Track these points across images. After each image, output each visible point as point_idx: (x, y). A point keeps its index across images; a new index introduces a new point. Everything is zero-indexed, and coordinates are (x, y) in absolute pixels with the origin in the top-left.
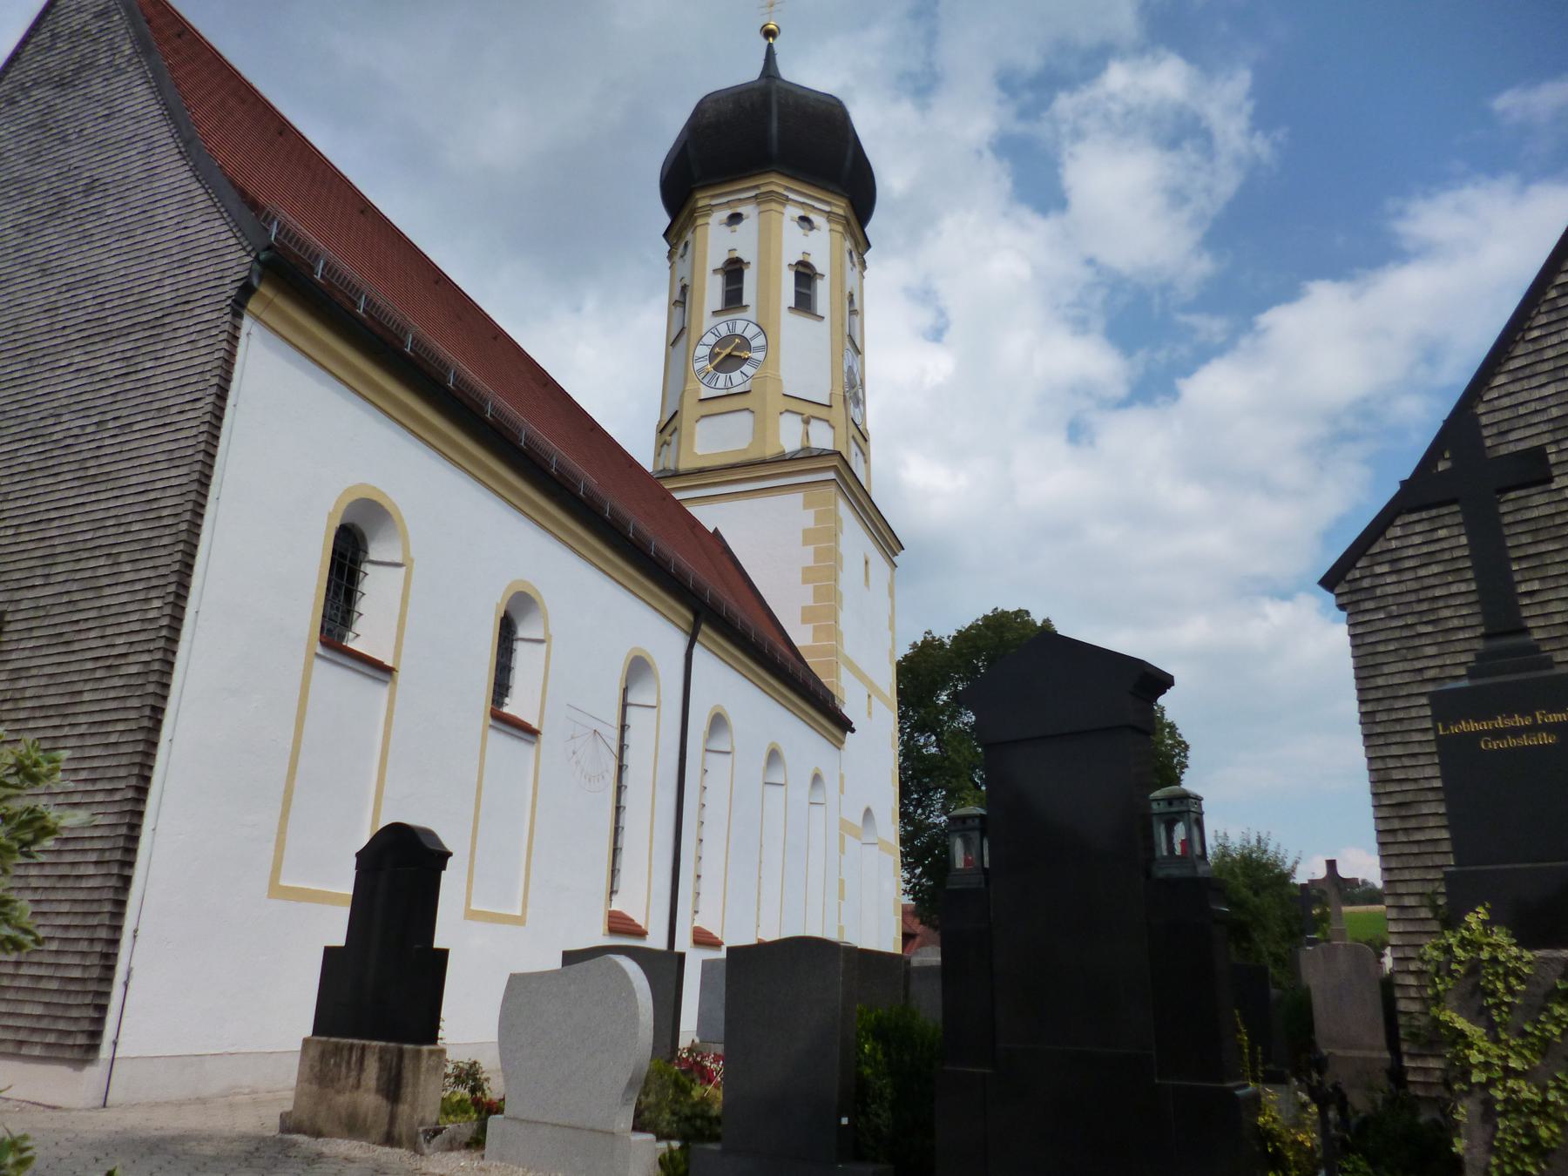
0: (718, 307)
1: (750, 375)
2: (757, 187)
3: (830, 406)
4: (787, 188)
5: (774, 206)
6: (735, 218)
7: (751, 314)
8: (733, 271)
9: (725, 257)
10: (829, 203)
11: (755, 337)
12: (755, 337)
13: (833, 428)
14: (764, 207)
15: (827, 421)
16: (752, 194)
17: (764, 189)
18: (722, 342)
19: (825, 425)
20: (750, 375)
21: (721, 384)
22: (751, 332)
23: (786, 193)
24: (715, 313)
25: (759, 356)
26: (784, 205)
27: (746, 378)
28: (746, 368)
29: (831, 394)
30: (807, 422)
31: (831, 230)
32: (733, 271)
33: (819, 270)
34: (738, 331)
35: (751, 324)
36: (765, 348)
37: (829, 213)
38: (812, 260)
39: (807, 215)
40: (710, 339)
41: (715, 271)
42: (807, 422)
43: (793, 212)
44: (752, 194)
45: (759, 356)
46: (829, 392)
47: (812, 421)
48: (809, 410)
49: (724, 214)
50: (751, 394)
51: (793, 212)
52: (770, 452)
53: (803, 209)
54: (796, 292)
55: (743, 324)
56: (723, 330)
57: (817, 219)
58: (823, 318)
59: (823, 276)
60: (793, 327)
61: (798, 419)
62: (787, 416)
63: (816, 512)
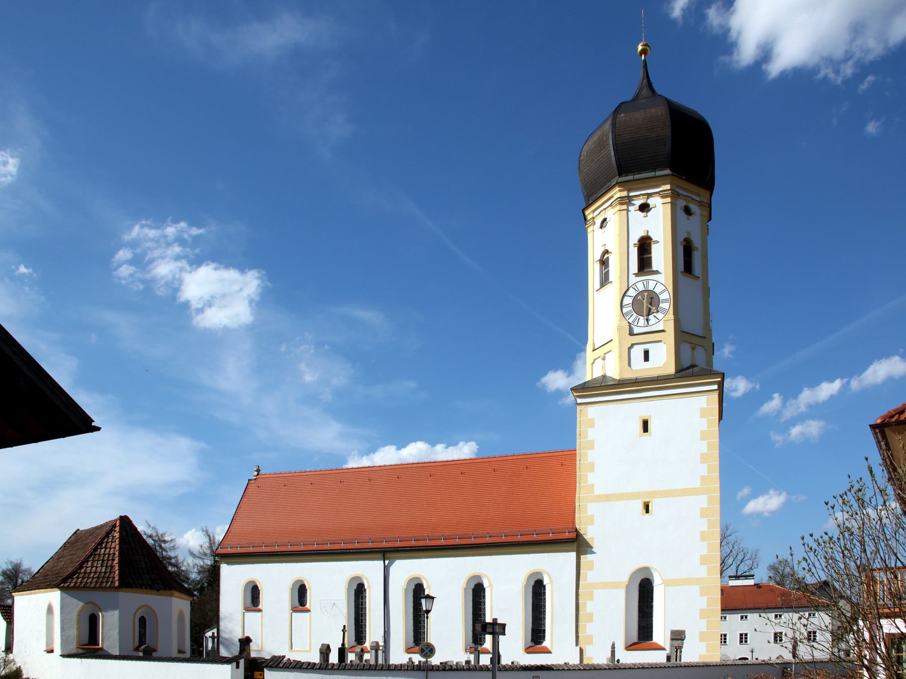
3: (704, 337)
6: (644, 208)
7: (660, 278)
8: (645, 245)
10: (699, 195)
11: (662, 292)
12: (662, 292)
13: (705, 350)
15: (703, 347)
27: (657, 321)
30: (693, 349)
32: (645, 245)
34: (651, 288)
37: (700, 202)
38: (692, 238)
39: (688, 205)
42: (693, 349)
49: (638, 202)
53: (686, 200)
54: (684, 260)
57: (694, 208)
58: (699, 278)
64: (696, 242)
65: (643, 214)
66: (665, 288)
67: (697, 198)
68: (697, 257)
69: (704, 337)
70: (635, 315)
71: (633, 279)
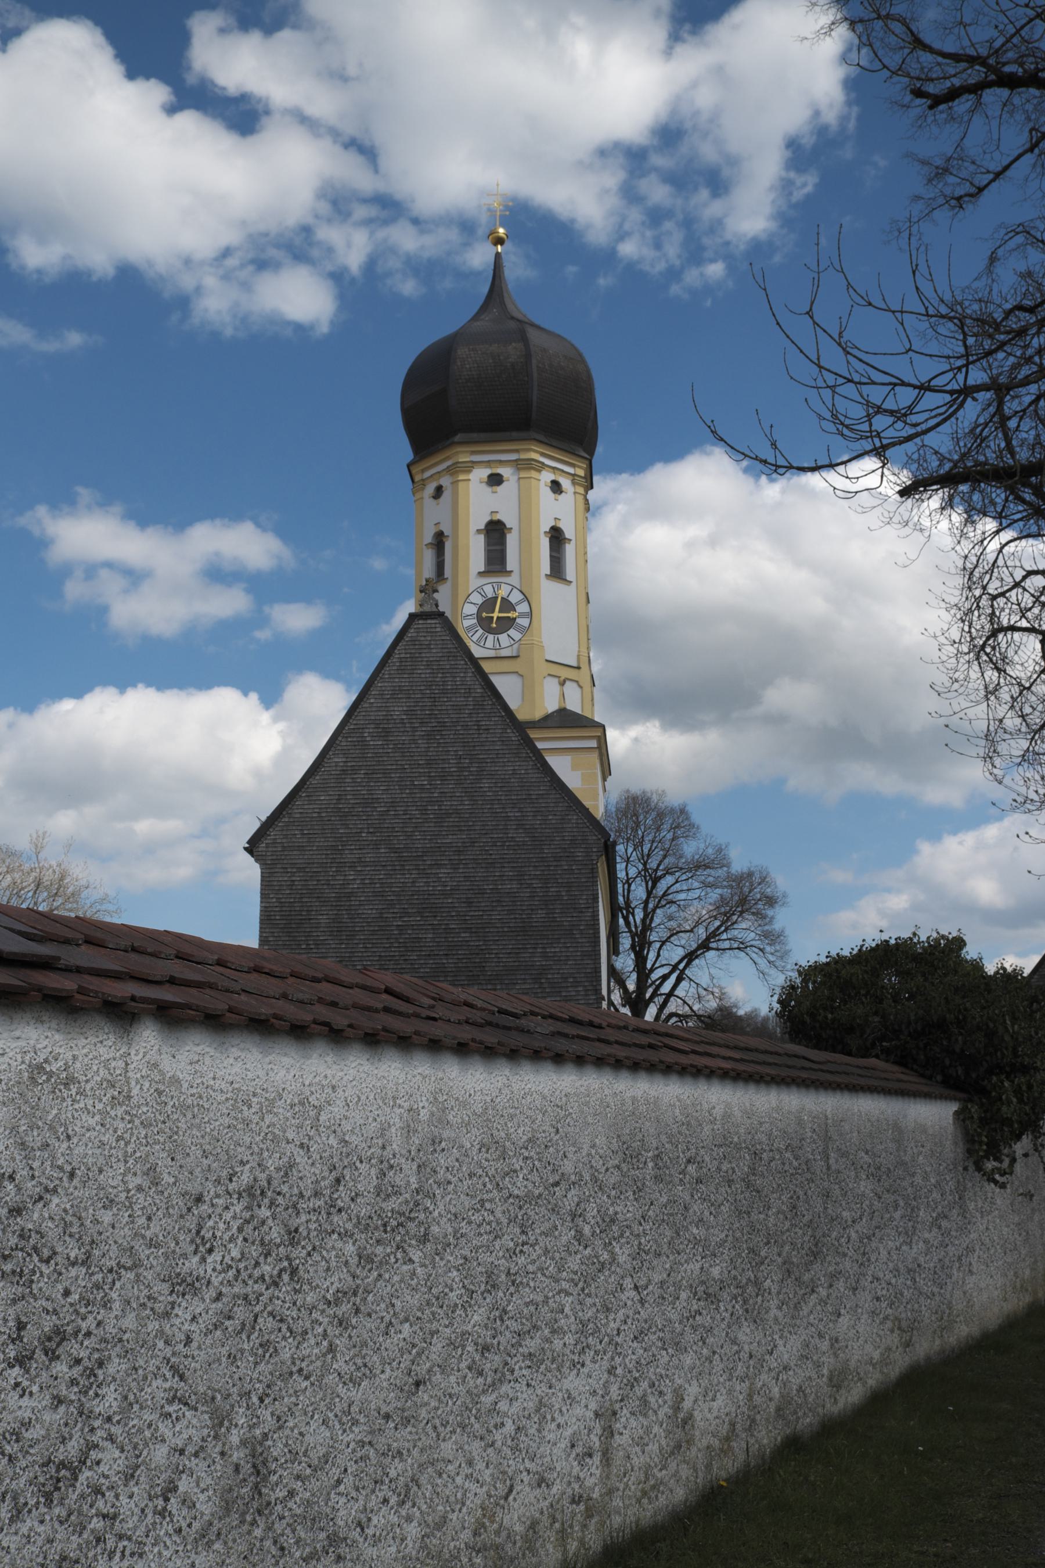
0: (482, 569)
1: (517, 639)
2: (517, 451)
3: (579, 668)
4: (543, 454)
5: (534, 474)
6: (495, 480)
7: (514, 579)
8: (495, 531)
9: (488, 519)
11: (519, 602)
12: (519, 602)
13: (581, 687)
14: (523, 474)
15: (577, 682)
16: (513, 457)
17: (524, 456)
18: (489, 604)
19: (575, 685)
20: (517, 639)
21: (489, 643)
22: (515, 597)
23: (542, 459)
24: (480, 574)
25: (524, 622)
26: (540, 471)
28: (512, 632)
29: (578, 656)
30: (562, 683)
31: (575, 493)
32: (495, 531)
33: (567, 536)
35: (515, 590)
36: (530, 615)
37: (574, 475)
38: (561, 525)
40: (478, 599)
41: (479, 531)
42: (562, 683)
43: (547, 477)
44: (513, 457)
45: (524, 622)
46: (576, 653)
47: (568, 683)
48: (565, 673)
49: (483, 473)
50: (519, 660)
51: (547, 477)
52: (538, 715)
54: (551, 556)
55: (505, 588)
56: (489, 592)
57: (565, 483)
59: (570, 540)
60: (549, 593)
61: (556, 680)
62: (550, 679)
63: (582, 774)
64: (569, 532)
65: (489, 489)
66: (522, 597)
67: (571, 470)
68: (570, 550)
69: (579, 668)
70: (481, 631)
71: (475, 582)
